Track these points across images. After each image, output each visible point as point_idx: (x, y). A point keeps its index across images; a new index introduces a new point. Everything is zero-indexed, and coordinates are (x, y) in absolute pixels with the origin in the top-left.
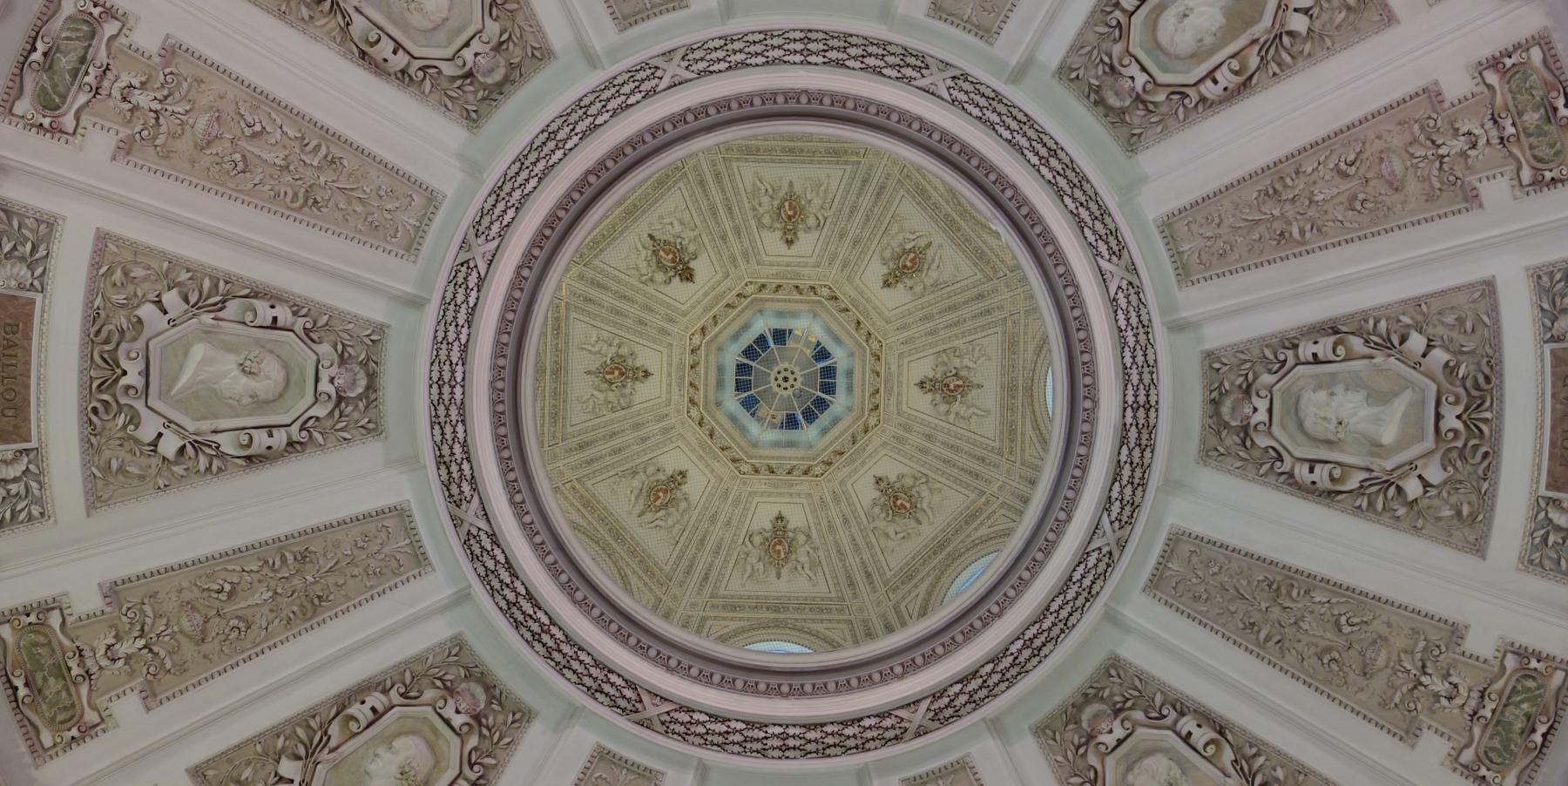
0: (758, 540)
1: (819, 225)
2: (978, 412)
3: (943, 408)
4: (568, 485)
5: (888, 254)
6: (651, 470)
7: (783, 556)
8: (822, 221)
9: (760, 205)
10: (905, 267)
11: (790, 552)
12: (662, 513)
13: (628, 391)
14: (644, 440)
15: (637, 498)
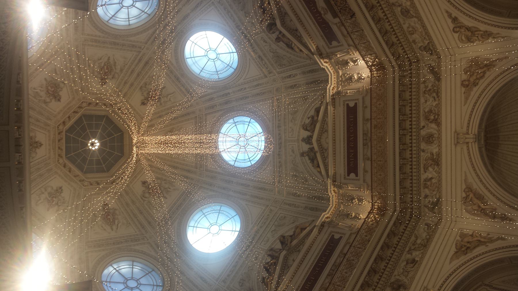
0: (62, 85)
1: (144, 197)
2: (40, 201)
3: (49, 190)
4: (143, 47)
5: (117, 212)
6: (116, 76)
7: (49, 88)
8: (144, 198)
9: (165, 183)
10: (109, 215)
11: (48, 91)
12: (103, 65)
13: (145, 94)
14: (125, 83)
15: (115, 63)
